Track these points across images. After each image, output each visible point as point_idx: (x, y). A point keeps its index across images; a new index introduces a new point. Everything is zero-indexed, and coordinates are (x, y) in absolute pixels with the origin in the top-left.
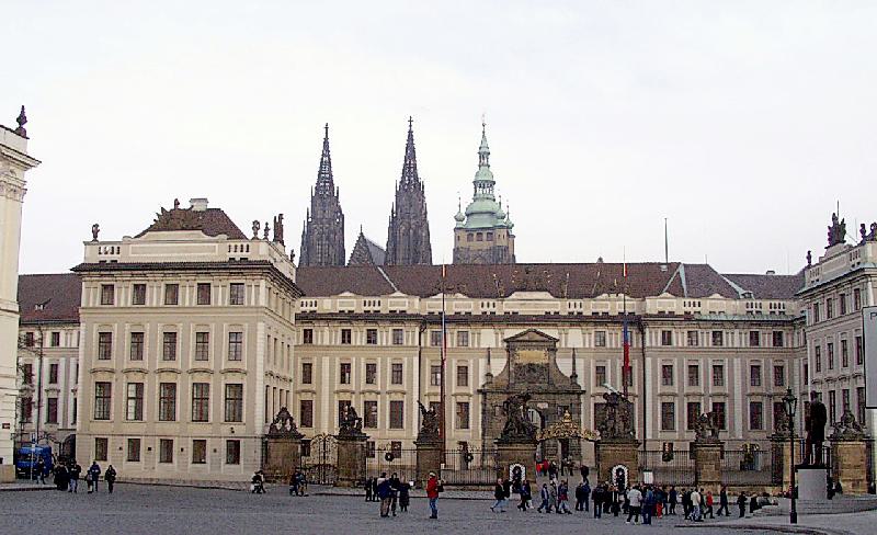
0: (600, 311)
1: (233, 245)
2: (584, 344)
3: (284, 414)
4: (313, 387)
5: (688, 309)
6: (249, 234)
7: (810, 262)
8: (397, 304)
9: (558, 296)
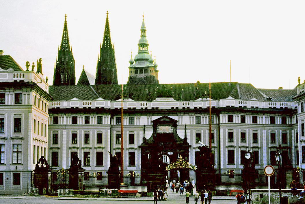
0: (198, 106)
1: (16, 73)
2: (190, 122)
3: (42, 160)
4: (58, 146)
5: (240, 105)
6: (24, 68)
7: (299, 82)
8: (100, 104)
9: (178, 99)
